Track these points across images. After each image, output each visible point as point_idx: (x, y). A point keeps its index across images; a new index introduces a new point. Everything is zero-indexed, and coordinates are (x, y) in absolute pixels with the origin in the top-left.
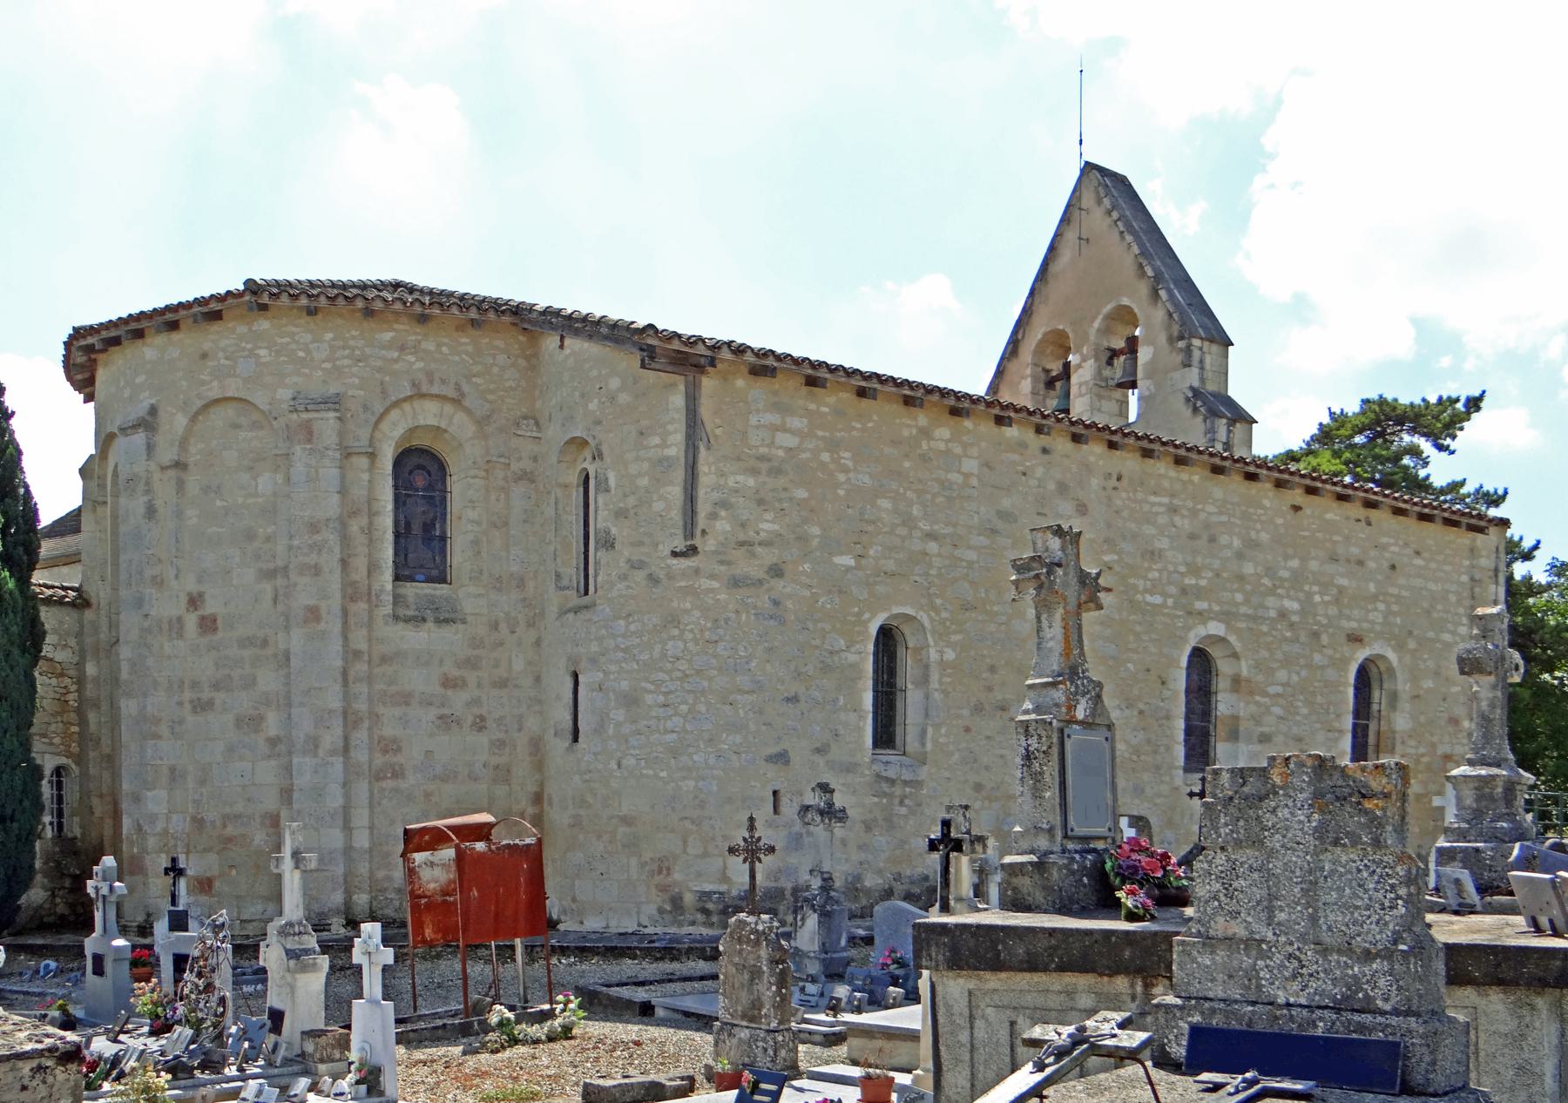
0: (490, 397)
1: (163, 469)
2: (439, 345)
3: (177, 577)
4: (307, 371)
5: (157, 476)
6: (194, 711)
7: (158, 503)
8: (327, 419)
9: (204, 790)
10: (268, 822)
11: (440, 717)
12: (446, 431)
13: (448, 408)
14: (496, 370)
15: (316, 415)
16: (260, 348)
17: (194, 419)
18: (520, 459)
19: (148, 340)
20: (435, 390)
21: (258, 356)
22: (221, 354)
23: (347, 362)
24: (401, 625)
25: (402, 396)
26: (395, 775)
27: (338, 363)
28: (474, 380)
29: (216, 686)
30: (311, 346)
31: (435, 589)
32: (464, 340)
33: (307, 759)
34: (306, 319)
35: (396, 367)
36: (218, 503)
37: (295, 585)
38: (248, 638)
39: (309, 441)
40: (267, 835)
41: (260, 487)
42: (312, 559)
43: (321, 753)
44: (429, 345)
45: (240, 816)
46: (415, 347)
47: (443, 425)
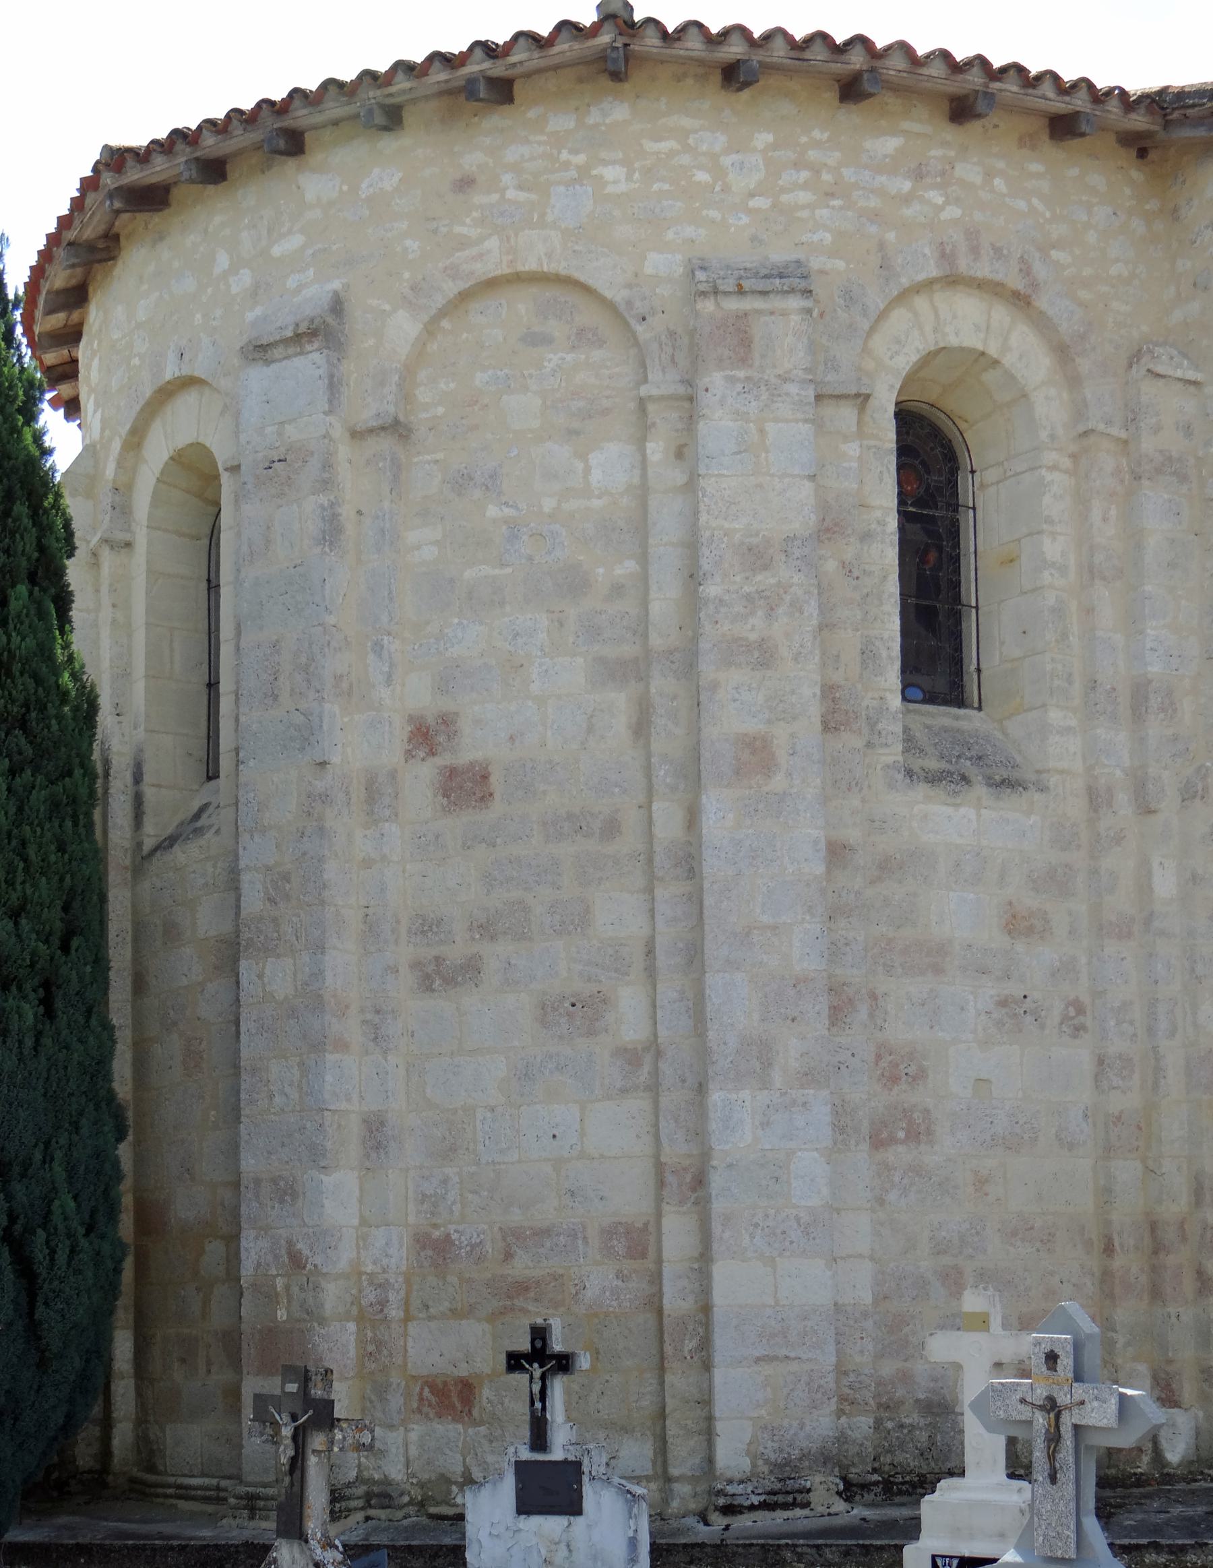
0: (1084, 295)
1: (357, 435)
2: (989, 175)
3: (389, 680)
4: (714, 214)
5: (344, 451)
6: (426, 984)
7: (347, 512)
8: (784, 314)
9: (450, 1171)
10: (620, 1247)
11: (1003, 1003)
12: (996, 363)
13: (1001, 314)
14: (1092, 237)
15: (758, 303)
16: (605, 163)
17: (431, 329)
18: (1157, 430)
19: (315, 157)
20: (983, 270)
21: (600, 182)
22: (507, 179)
23: (804, 197)
24: (922, 789)
25: (921, 277)
26: (915, 1135)
27: (784, 198)
28: (1054, 254)
29: (486, 929)
30: (727, 161)
31: (957, 718)
32: (1036, 167)
33: (746, 1094)
34: (714, 98)
35: (908, 212)
36: (492, 511)
37: (714, 686)
38: (570, 816)
39: (744, 361)
40: (619, 1275)
41: (596, 476)
42: (754, 627)
43: (778, 1079)
44: (969, 172)
45: (546, 1232)
46: (943, 173)
47: (993, 350)
